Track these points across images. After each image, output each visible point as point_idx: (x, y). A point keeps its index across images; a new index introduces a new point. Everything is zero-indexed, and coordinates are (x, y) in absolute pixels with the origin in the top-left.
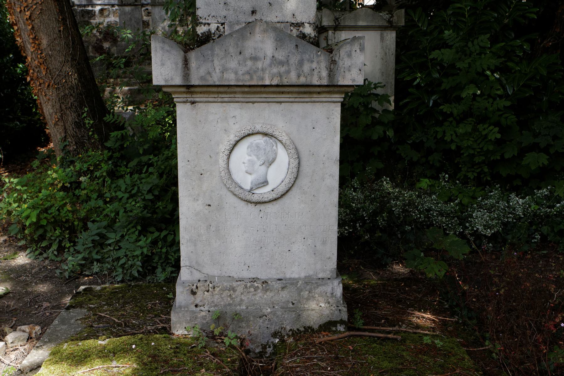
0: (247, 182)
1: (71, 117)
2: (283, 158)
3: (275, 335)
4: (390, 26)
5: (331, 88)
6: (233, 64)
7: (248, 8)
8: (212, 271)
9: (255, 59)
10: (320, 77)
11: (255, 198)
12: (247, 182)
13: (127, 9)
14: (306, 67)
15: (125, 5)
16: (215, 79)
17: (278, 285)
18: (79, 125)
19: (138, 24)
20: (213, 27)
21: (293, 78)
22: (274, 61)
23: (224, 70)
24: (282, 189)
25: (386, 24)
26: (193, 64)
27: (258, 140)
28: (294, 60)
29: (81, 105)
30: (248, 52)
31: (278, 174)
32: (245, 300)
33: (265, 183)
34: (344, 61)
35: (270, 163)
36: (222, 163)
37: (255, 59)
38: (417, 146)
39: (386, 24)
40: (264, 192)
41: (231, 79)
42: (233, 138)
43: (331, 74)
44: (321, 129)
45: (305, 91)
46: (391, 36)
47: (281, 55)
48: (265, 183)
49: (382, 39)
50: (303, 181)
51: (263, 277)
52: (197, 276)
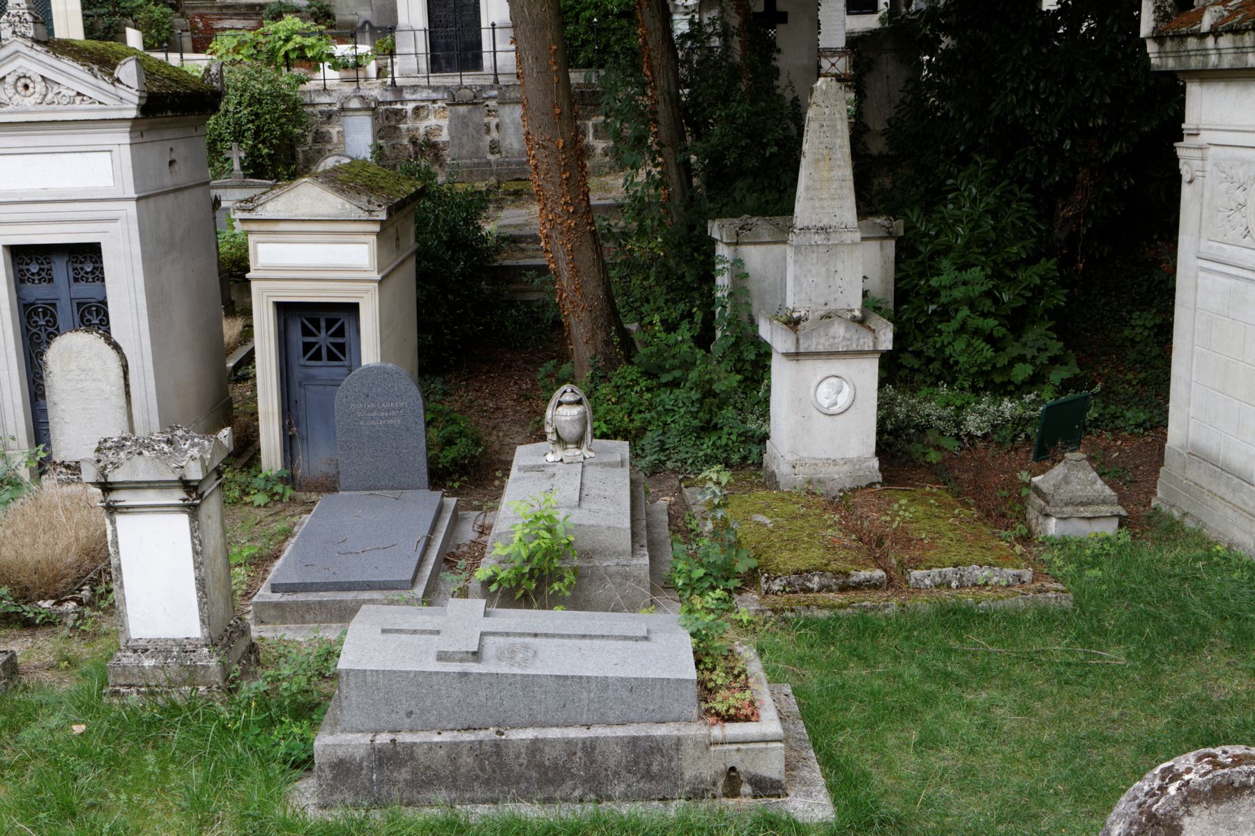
0: (826, 403)
1: (601, 336)
2: (847, 389)
3: (840, 491)
4: (890, 236)
5: (874, 352)
6: (822, 341)
7: (822, 301)
8: (805, 454)
9: (834, 338)
10: (867, 344)
11: (830, 412)
12: (826, 403)
13: (462, 109)
14: (861, 341)
15: (458, 104)
16: (813, 349)
17: (842, 462)
18: (608, 343)
19: (478, 132)
20: (802, 314)
21: (854, 347)
22: (844, 339)
23: (818, 344)
24: (846, 407)
25: (885, 235)
26: (801, 341)
27: (834, 380)
28: (855, 337)
29: (610, 325)
30: (831, 334)
31: (843, 400)
32: (823, 472)
33: (836, 404)
34: (882, 337)
35: (839, 392)
36: (812, 392)
37: (834, 338)
38: (918, 354)
39: (885, 235)
40: (835, 409)
41: (821, 349)
42: (819, 379)
43: (875, 345)
44: (867, 373)
45: (860, 353)
46: (891, 246)
47: (848, 336)
48: (836, 404)
49: (882, 247)
50: (857, 402)
51: (833, 457)
52: (796, 457)
